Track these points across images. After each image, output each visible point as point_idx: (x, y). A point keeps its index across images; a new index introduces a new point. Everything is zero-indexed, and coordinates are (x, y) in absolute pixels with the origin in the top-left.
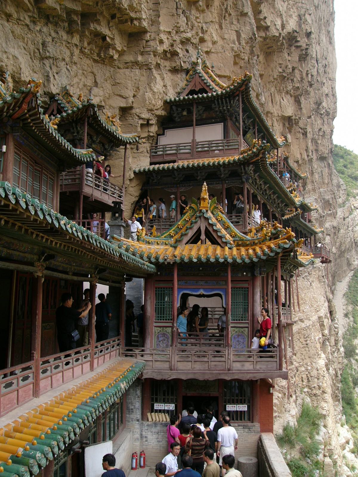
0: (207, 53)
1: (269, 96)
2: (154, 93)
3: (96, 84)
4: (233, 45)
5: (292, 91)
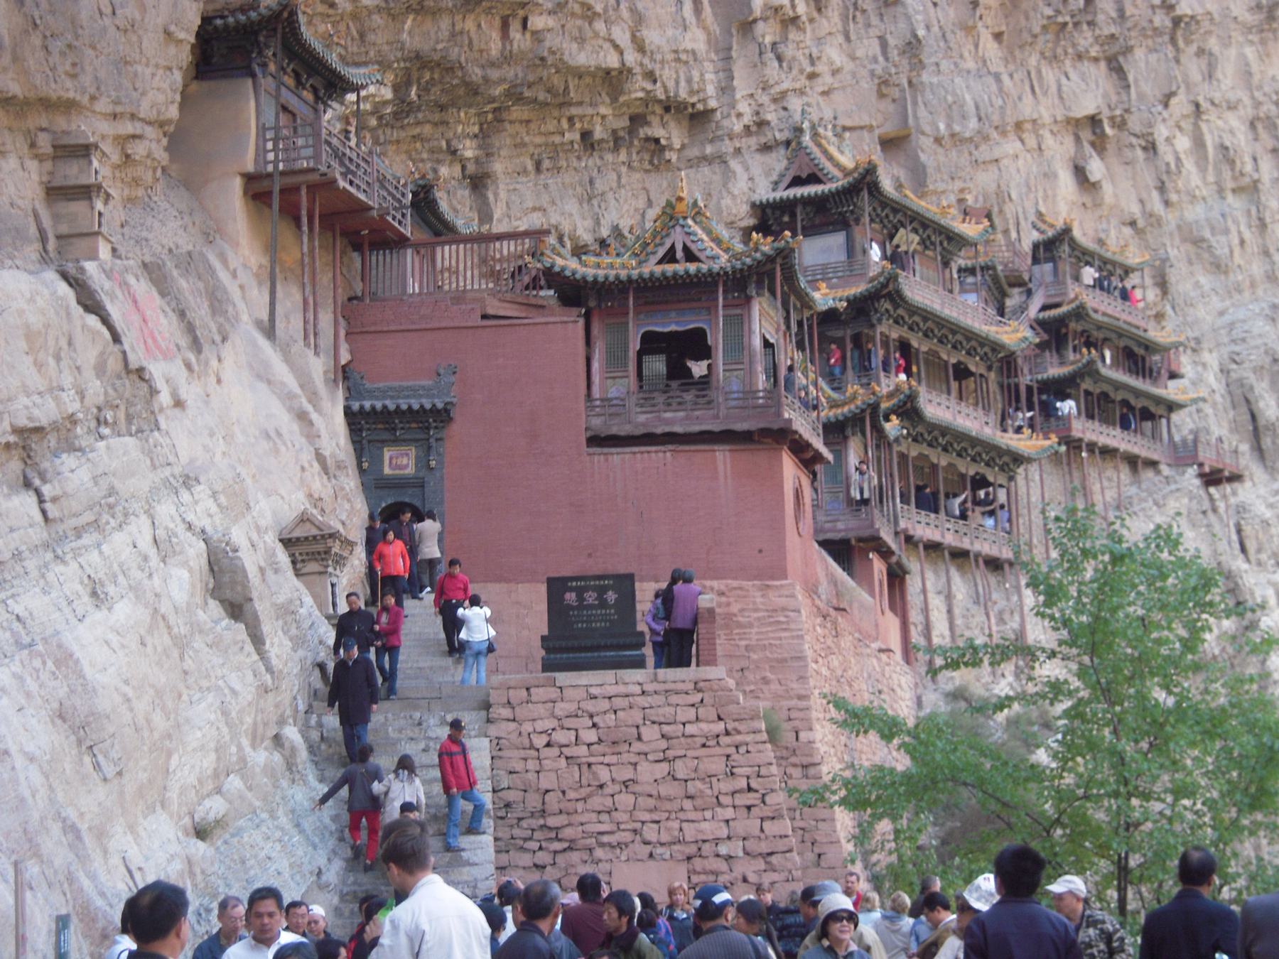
0: (825, 93)
1: (1022, 81)
2: (734, 197)
3: (650, 203)
4: (874, 66)
5: (1097, 48)
